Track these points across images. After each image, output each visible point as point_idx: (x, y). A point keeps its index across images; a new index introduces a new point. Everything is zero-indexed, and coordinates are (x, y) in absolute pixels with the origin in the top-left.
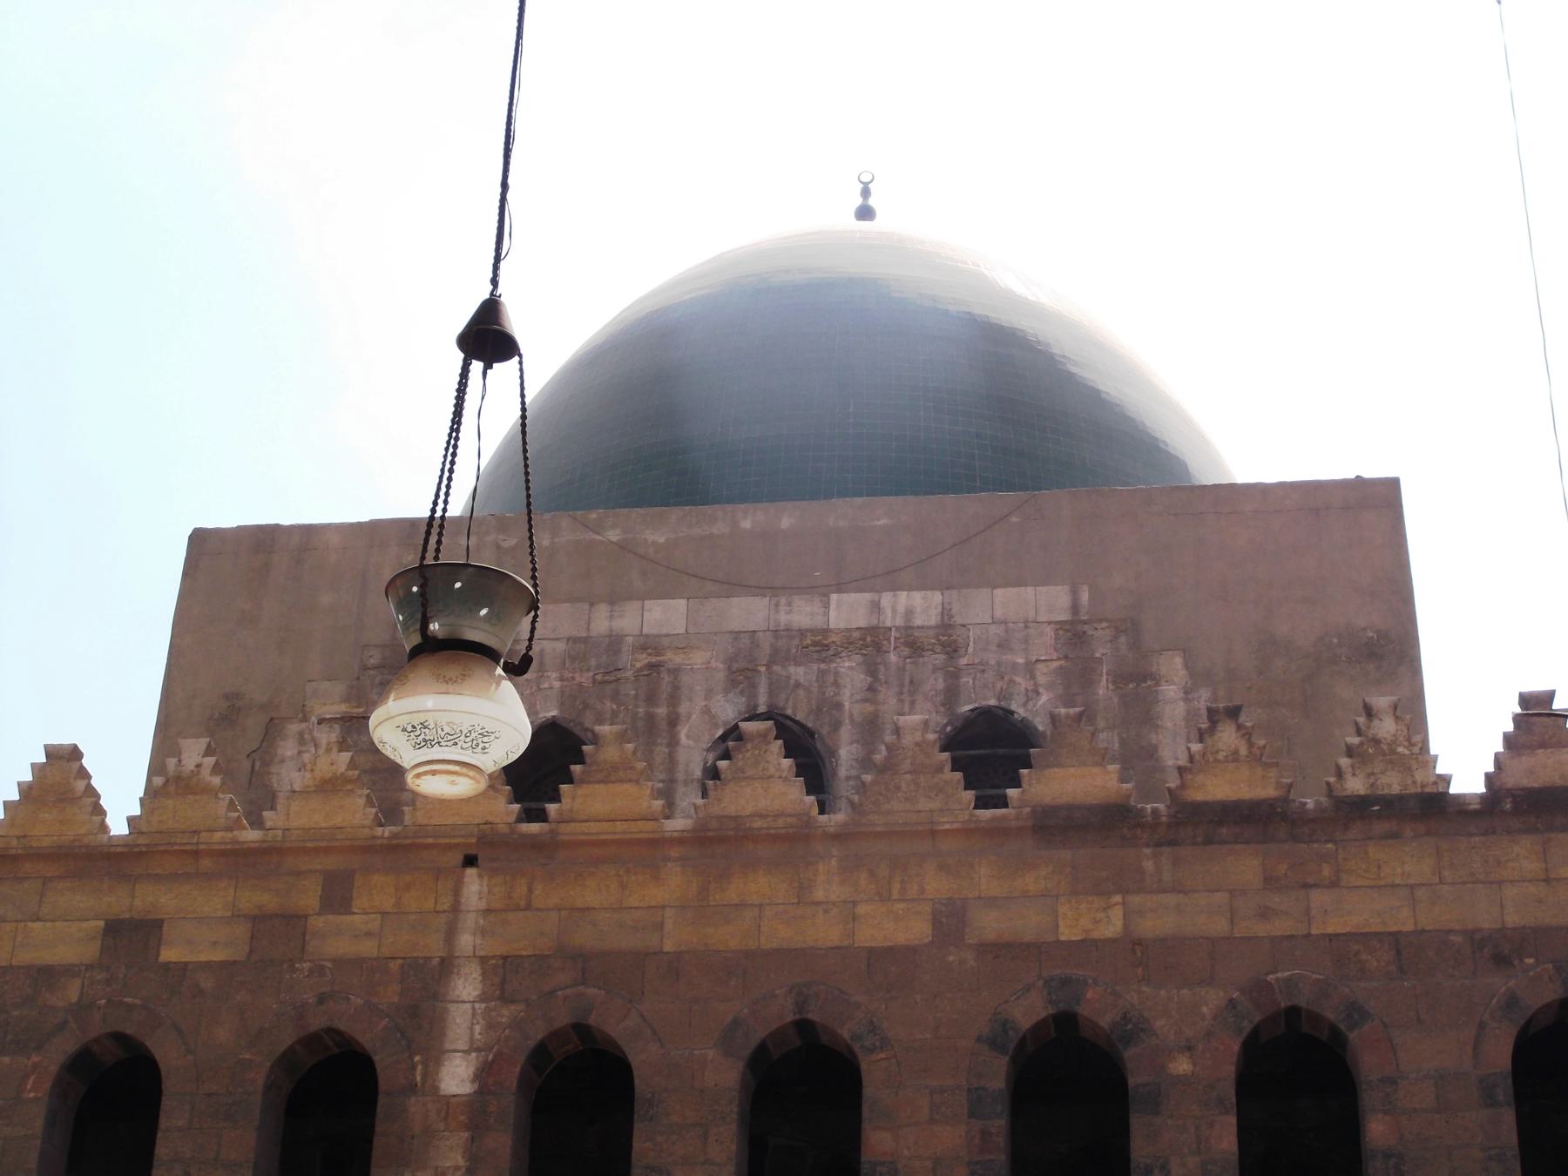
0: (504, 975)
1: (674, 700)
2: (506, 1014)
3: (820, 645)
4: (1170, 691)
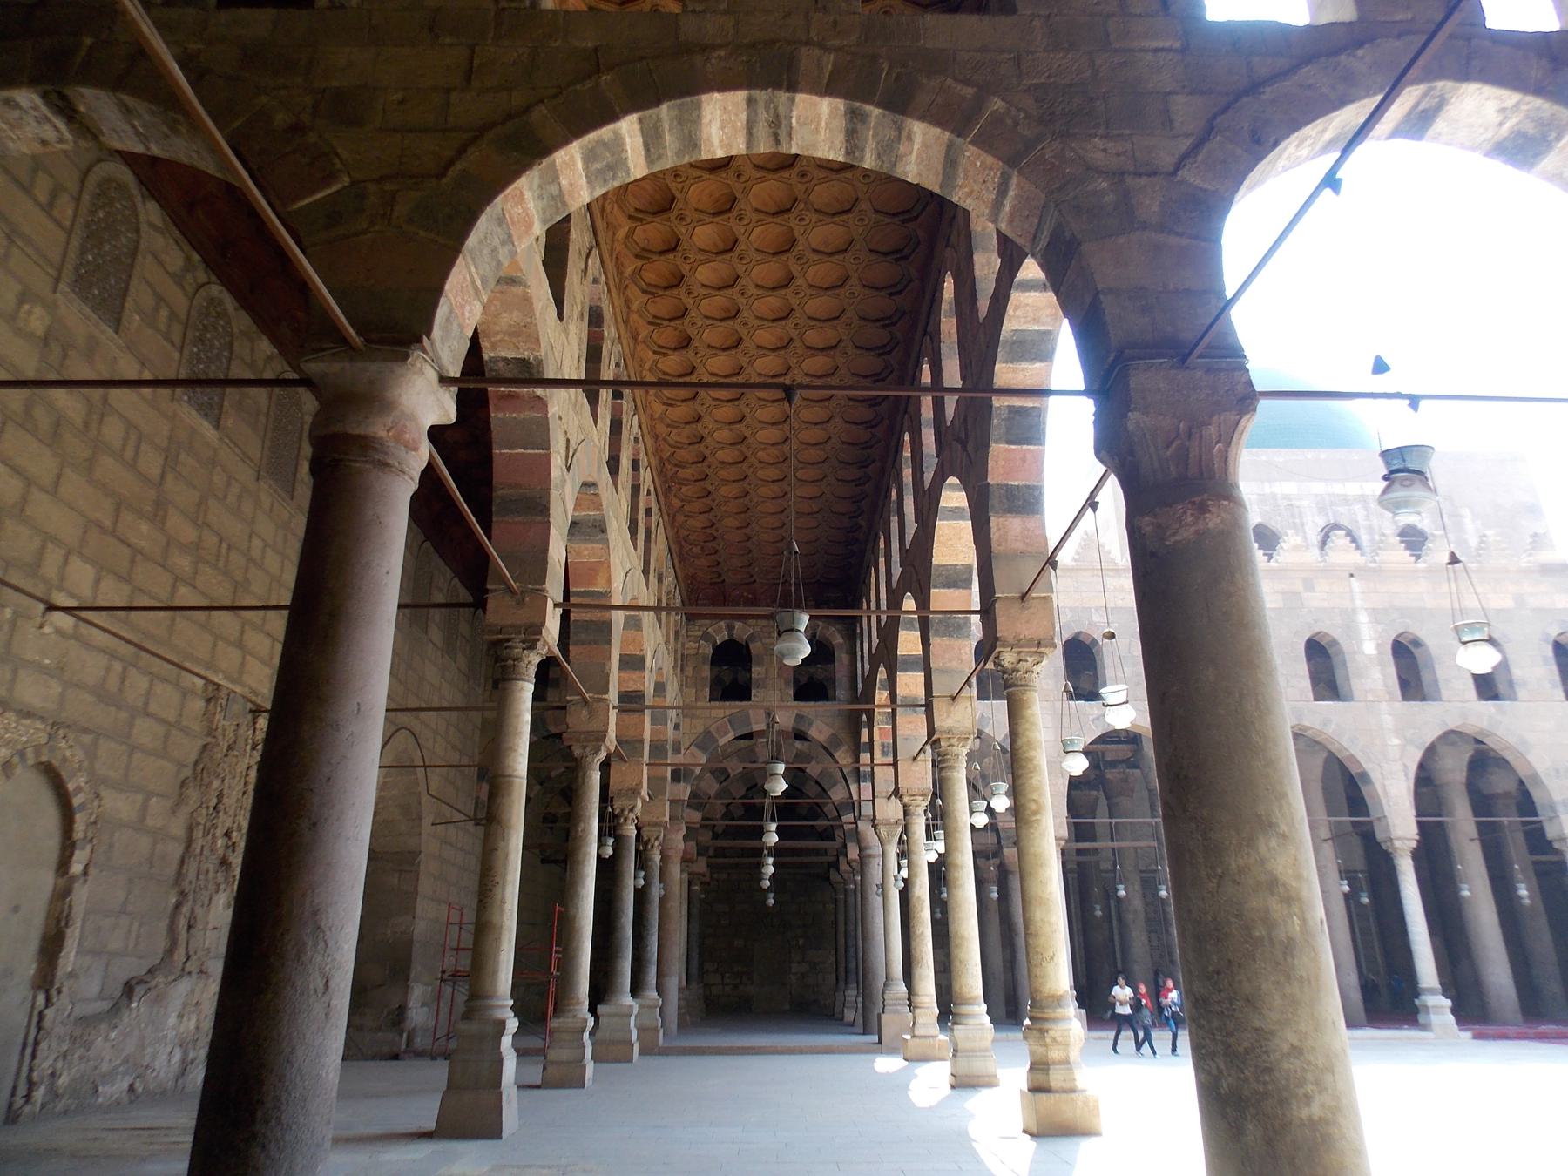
0: (1376, 615)
1: (1300, 514)
2: (1380, 628)
3: (1346, 500)
4: (1468, 521)
